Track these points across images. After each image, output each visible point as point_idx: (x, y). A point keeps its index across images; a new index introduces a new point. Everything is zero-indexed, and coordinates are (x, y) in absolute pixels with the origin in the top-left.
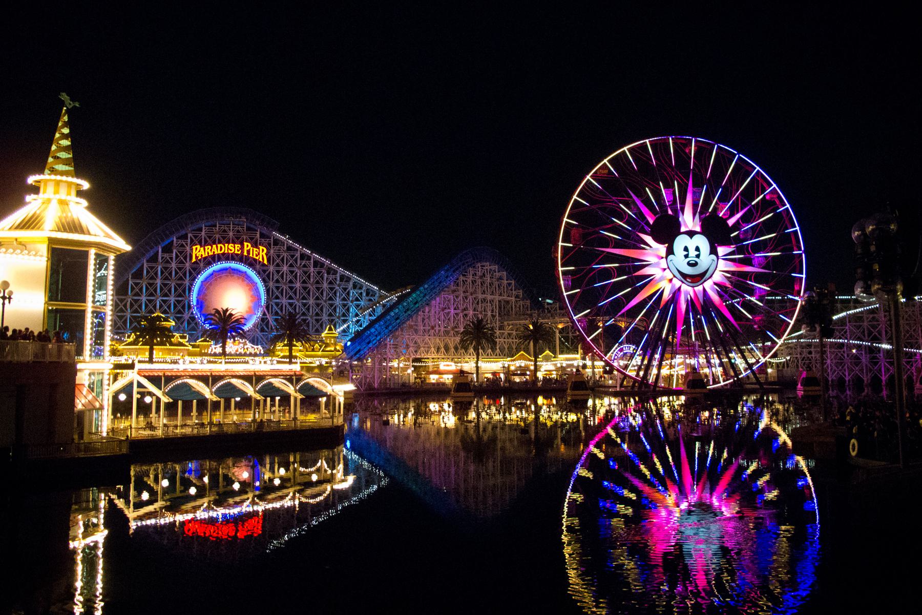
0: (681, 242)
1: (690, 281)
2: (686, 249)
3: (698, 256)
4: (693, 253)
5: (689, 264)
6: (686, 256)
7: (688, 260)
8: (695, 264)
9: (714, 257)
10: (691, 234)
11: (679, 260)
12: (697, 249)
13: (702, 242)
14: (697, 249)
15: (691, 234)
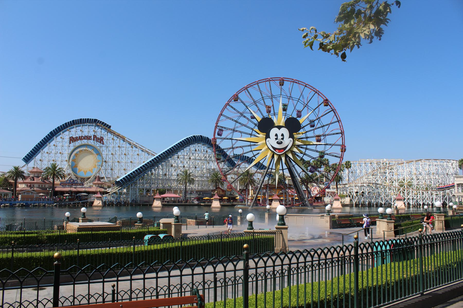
0: (274, 131)
1: (278, 151)
2: (276, 135)
3: (283, 139)
4: (280, 137)
5: (278, 143)
6: (276, 139)
7: (277, 141)
8: (281, 143)
9: (291, 139)
10: (279, 127)
11: (272, 142)
12: (282, 135)
13: (285, 131)
14: (282, 135)
15: (279, 127)
